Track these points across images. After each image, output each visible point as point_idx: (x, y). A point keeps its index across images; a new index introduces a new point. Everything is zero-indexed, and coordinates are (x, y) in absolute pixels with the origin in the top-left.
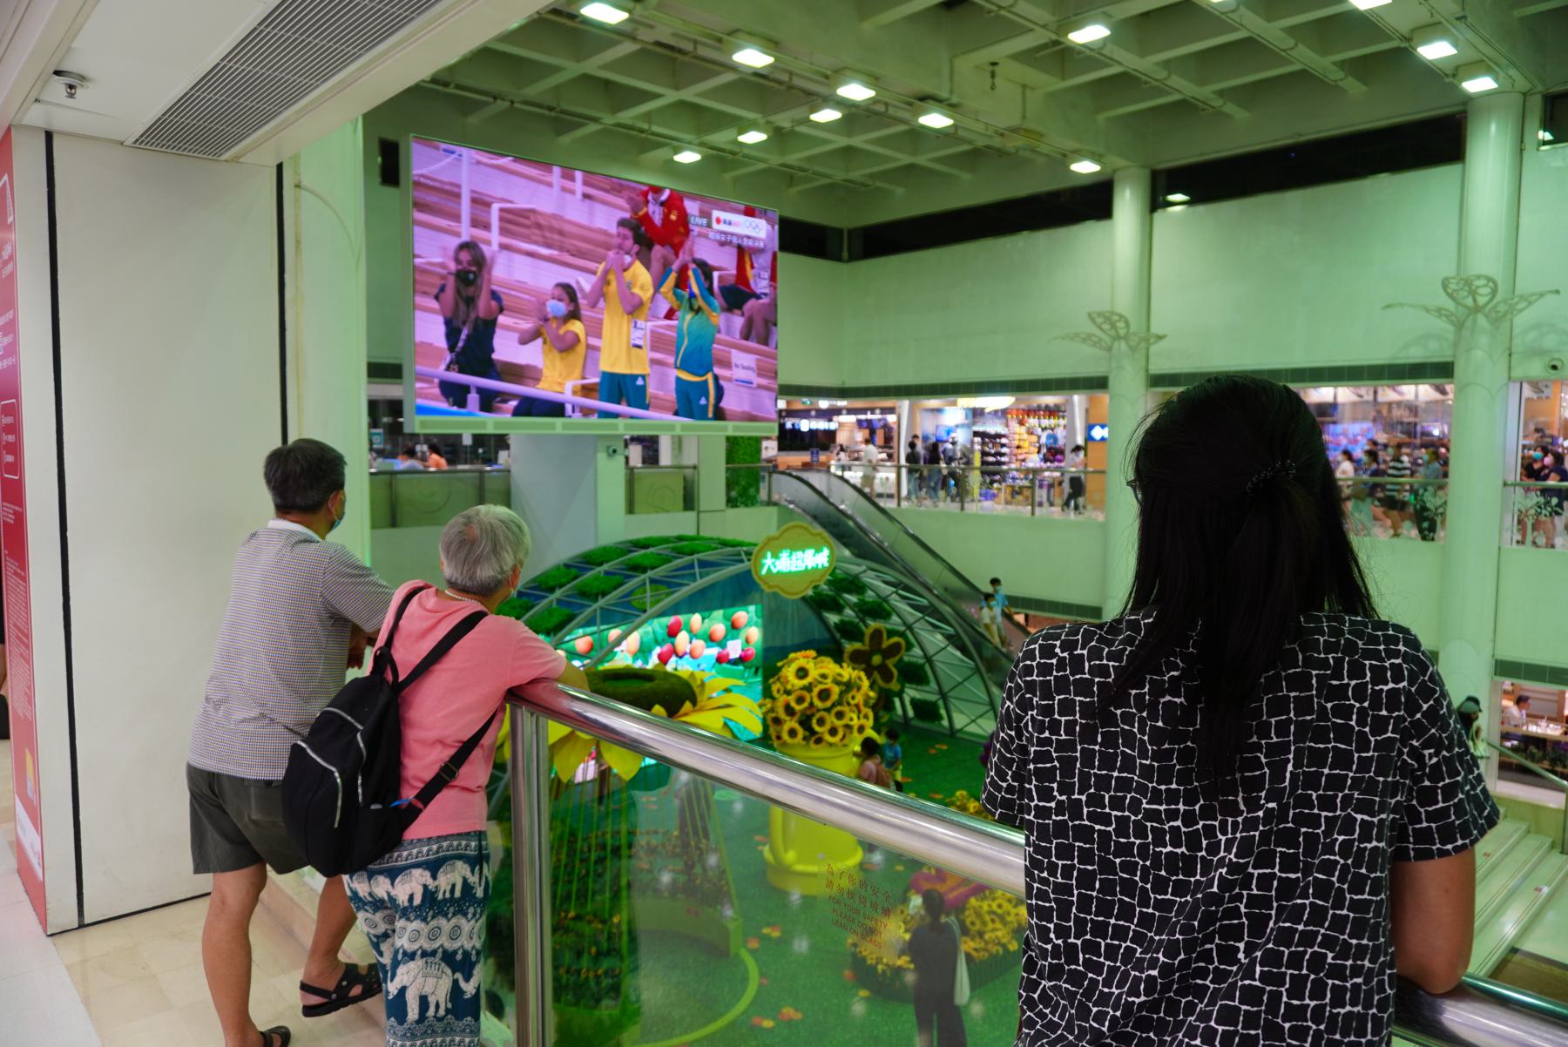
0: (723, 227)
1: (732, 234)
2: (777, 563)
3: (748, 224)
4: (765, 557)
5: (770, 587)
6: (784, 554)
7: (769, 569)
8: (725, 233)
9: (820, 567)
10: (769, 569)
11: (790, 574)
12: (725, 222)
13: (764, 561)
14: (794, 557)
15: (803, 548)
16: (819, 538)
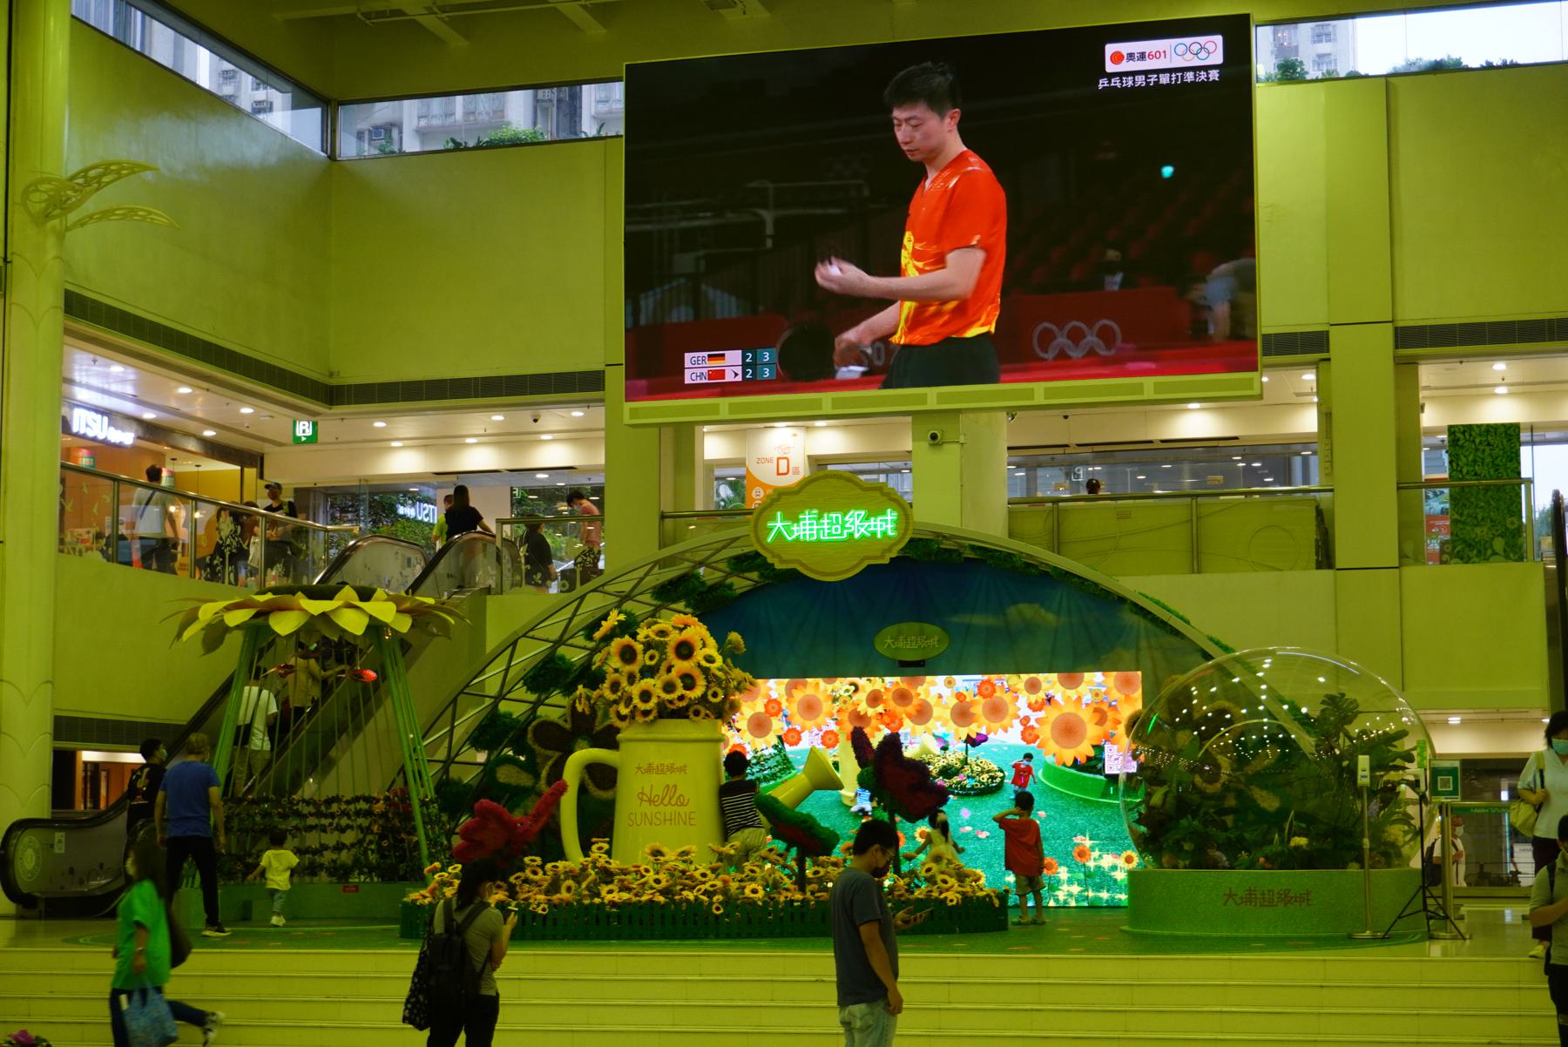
1: (1158, 72)
2: (795, 527)
3: (1181, 49)
4: (774, 519)
6: (808, 517)
7: (779, 535)
8: (1146, 73)
9: (879, 536)
10: (779, 535)
11: (819, 542)
13: (770, 524)
15: (844, 508)
16: (877, 494)
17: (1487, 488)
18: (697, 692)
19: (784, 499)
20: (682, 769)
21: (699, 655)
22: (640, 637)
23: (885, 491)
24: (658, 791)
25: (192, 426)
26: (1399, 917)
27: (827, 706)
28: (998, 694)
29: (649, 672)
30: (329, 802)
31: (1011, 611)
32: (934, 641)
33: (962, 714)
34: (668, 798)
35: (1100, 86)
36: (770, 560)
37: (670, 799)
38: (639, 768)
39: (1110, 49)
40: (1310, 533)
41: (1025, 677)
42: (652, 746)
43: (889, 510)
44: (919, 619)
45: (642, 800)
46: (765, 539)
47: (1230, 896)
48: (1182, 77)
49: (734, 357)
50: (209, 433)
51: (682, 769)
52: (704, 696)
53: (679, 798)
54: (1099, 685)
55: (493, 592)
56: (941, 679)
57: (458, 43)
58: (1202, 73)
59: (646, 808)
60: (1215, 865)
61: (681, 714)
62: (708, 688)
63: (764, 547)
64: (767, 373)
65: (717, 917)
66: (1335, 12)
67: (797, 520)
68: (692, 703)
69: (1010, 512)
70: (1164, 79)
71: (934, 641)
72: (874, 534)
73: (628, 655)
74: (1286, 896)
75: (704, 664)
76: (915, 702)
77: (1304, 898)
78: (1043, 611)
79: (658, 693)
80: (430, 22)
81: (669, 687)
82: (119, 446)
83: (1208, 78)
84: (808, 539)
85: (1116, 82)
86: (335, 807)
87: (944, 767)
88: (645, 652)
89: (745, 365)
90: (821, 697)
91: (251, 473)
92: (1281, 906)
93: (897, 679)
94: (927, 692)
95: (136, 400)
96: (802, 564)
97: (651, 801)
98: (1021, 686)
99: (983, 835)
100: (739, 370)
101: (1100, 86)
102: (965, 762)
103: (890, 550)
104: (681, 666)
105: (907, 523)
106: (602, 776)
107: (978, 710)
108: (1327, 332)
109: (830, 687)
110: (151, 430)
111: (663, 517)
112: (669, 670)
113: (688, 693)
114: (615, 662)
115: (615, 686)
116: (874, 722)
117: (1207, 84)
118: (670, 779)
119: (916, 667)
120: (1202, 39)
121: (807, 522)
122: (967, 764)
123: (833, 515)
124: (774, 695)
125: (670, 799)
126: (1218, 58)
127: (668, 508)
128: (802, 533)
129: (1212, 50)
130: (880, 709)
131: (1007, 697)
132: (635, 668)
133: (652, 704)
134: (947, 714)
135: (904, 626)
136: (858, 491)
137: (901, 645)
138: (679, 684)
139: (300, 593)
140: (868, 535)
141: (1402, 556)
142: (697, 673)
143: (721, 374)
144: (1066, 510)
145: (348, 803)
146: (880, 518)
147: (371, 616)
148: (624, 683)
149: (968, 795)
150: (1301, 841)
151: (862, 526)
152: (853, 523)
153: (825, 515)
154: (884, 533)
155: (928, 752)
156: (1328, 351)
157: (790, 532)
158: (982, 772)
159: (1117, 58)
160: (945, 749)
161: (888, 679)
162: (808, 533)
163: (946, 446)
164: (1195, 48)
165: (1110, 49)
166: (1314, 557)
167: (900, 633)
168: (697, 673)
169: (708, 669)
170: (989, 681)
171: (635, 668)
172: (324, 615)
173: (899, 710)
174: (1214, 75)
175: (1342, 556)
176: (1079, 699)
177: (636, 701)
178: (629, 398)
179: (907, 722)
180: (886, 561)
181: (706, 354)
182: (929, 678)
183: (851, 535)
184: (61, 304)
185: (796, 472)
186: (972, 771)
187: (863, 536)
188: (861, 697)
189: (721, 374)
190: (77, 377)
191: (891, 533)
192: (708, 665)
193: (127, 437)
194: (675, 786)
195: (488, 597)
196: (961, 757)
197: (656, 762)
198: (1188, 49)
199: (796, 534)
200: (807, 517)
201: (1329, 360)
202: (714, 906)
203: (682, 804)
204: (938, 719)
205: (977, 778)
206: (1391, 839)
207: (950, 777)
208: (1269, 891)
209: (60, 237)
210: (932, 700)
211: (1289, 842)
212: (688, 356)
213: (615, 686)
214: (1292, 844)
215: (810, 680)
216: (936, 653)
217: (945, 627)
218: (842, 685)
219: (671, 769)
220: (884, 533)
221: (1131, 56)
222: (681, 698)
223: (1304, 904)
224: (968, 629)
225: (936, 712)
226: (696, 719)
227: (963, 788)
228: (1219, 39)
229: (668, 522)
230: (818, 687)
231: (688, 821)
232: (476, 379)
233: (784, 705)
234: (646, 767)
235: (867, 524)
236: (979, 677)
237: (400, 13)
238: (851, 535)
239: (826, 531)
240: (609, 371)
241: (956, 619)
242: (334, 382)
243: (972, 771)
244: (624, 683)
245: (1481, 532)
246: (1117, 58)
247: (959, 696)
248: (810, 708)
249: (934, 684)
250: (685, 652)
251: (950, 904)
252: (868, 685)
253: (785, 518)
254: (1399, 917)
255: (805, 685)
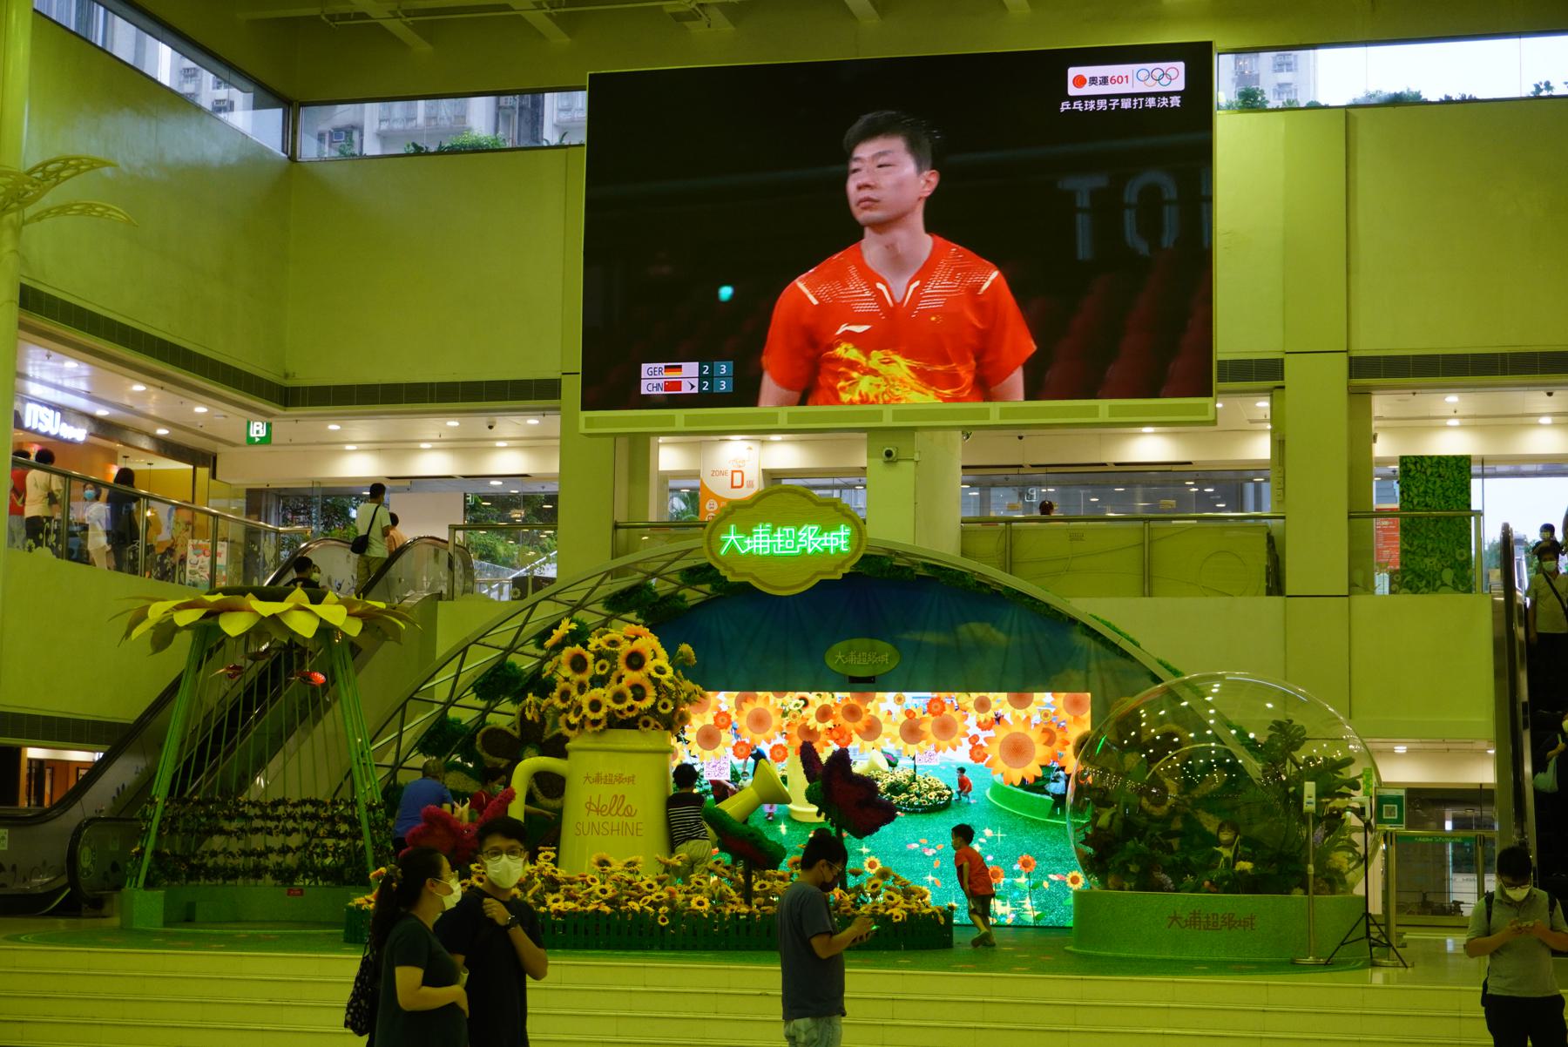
0: (1088, 90)
2: (748, 541)
3: (1143, 75)
4: (728, 532)
5: (734, 574)
7: (733, 548)
8: (1108, 97)
9: (832, 552)
11: (772, 557)
12: (1093, 80)
14: (779, 535)
16: (831, 509)
17: (1437, 520)
18: (648, 703)
19: (738, 512)
20: (631, 780)
21: (650, 666)
22: (592, 646)
23: (839, 506)
24: (606, 800)
25: (145, 424)
26: (1342, 944)
27: (776, 720)
28: (947, 712)
29: (599, 681)
30: (275, 804)
31: (963, 629)
32: (885, 658)
33: (911, 732)
34: (615, 808)
35: (1062, 109)
36: (723, 573)
37: (618, 809)
38: (587, 778)
39: (1073, 72)
40: (1262, 560)
41: (974, 695)
42: (601, 756)
43: (842, 526)
44: (872, 634)
45: (589, 809)
46: (719, 552)
47: (1175, 918)
48: (1144, 102)
49: (690, 369)
50: (162, 432)
51: (631, 780)
52: (654, 707)
53: (626, 808)
54: (1049, 705)
55: (444, 597)
56: (890, 696)
57: (422, 48)
58: (1164, 99)
59: (594, 818)
60: (1160, 887)
61: (630, 724)
62: (658, 699)
63: (717, 560)
64: (723, 386)
65: (662, 928)
66: (1296, 42)
67: (749, 533)
68: (642, 713)
69: (963, 531)
70: (1126, 104)
71: (885, 658)
72: (827, 549)
73: (578, 664)
74: (1230, 920)
75: (655, 674)
76: (865, 718)
77: (1248, 923)
78: (993, 631)
79: (608, 702)
80: (395, 26)
81: (619, 697)
82: (71, 443)
83: (1169, 104)
84: (761, 553)
85: (1078, 105)
86: (281, 810)
87: (892, 783)
88: (595, 661)
89: (701, 378)
90: (771, 711)
91: (203, 472)
92: (1225, 929)
93: (848, 695)
94: (877, 709)
95: (89, 396)
96: (756, 579)
97: (598, 811)
98: (971, 705)
99: (930, 853)
100: (695, 382)
101: (1062, 109)
102: (913, 779)
103: (842, 565)
104: (632, 676)
105: (860, 539)
106: (550, 785)
107: (927, 727)
108: (1282, 360)
109: (779, 701)
110: (104, 427)
111: (616, 527)
112: (619, 680)
113: (634, 702)
114: (566, 671)
115: (565, 695)
116: (823, 738)
117: (1168, 110)
118: (619, 789)
119: (866, 683)
120: (1164, 66)
121: (761, 535)
122: (915, 781)
123: (787, 529)
124: (724, 708)
125: (618, 809)
126: (1179, 85)
127: (621, 518)
128: (755, 546)
129: (1173, 76)
130: (829, 724)
131: (957, 716)
132: (586, 677)
133: (601, 714)
134: (896, 731)
135: (856, 642)
136: (812, 506)
137: (852, 660)
138: (629, 694)
139: (250, 594)
140: (822, 550)
141: (1352, 585)
142: (647, 684)
143: (678, 385)
144: (1019, 530)
145: (294, 806)
146: (833, 534)
147: (321, 619)
148: (574, 693)
149: (915, 812)
150: (1245, 866)
151: (815, 541)
152: (806, 538)
153: (779, 529)
154: (838, 549)
155: (876, 768)
156: (1283, 379)
157: (743, 546)
158: (930, 790)
159: (1080, 81)
160: (892, 764)
161: (838, 695)
162: (761, 546)
163: (901, 464)
164: (1157, 74)
165: (1073, 72)
166: (1264, 584)
167: (850, 649)
168: (647, 684)
169: (659, 680)
170: (938, 699)
171: (586, 677)
172: (274, 616)
173: (849, 726)
174: (1176, 101)
175: (1290, 588)
176: (1028, 719)
177: (586, 710)
178: (584, 409)
179: (856, 737)
180: (839, 576)
181: (662, 365)
182: (879, 695)
183: (804, 550)
184: (17, 298)
185: (750, 485)
186: (920, 788)
187: (816, 551)
188: (811, 711)
189: (678, 385)
190: (30, 372)
191: (844, 549)
192: (658, 676)
193: (79, 434)
194: (623, 796)
195: (439, 602)
196: (910, 774)
197: (604, 771)
198: (1151, 75)
199: (749, 548)
200: (761, 530)
201: (1283, 387)
202: (660, 918)
203: (630, 815)
204: (887, 736)
205: (925, 796)
206: (1336, 865)
207: (898, 794)
208: (1213, 914)
209: (17, 230)
210: (881, 717)
211: (1234, 866)
212: (645, 367)
213: (565, 695)
214: (1237, 868)
215: (759, 694)
216: (885, 670)
217: (896, 644)
218: (791, 699)
219: (620, 779)
220: (838, 549)
221: (1093, 80)
222: (631, 708)
223: (1249, 928)
224: (919, 645)
225: (886, 728)
226: (645, 729)
227: (911, 805)
228: (1181, 66)
229: (621, 532)
230: (768, 701)
231: (635, 832)
232: (432, 384)
233: (734, 717)
234: (594, 776)
235: (820, 539)
236: (929, 694)
237: (364, 16)
238: (804, 550)
239: (780, 546)
240: (565, 381)
241: (906, 636)
242: (290, 383)
243: (920, 788)
244: (574, 693)
245: (1430, 563)
246: (1080, 81)
247: (909, 713)
248: (759, 721)
249: (883, 700)
250: (635, 662)
251: (895, 920)
252: (817, 700)
253: (738, 532)
254: (1342, 944)
255: (755, 698)
